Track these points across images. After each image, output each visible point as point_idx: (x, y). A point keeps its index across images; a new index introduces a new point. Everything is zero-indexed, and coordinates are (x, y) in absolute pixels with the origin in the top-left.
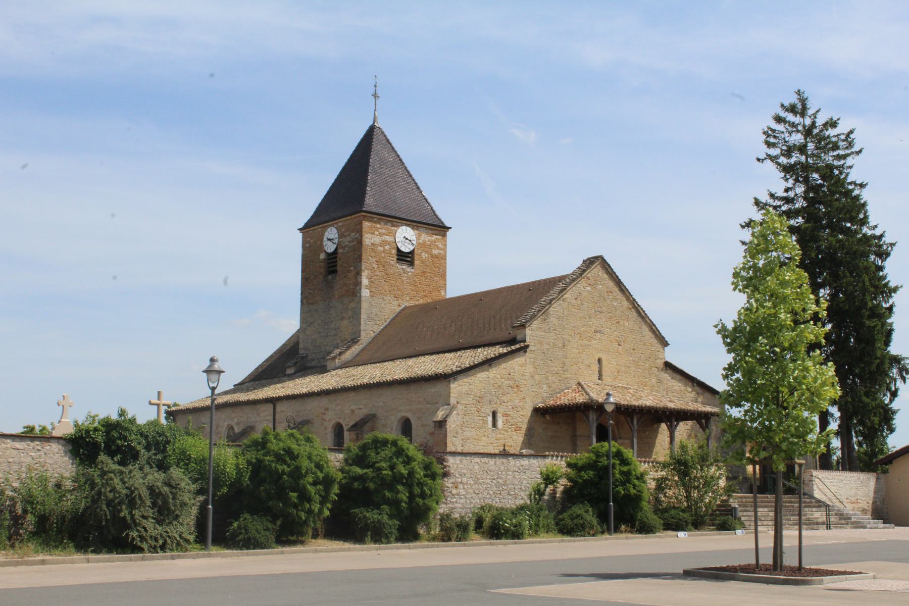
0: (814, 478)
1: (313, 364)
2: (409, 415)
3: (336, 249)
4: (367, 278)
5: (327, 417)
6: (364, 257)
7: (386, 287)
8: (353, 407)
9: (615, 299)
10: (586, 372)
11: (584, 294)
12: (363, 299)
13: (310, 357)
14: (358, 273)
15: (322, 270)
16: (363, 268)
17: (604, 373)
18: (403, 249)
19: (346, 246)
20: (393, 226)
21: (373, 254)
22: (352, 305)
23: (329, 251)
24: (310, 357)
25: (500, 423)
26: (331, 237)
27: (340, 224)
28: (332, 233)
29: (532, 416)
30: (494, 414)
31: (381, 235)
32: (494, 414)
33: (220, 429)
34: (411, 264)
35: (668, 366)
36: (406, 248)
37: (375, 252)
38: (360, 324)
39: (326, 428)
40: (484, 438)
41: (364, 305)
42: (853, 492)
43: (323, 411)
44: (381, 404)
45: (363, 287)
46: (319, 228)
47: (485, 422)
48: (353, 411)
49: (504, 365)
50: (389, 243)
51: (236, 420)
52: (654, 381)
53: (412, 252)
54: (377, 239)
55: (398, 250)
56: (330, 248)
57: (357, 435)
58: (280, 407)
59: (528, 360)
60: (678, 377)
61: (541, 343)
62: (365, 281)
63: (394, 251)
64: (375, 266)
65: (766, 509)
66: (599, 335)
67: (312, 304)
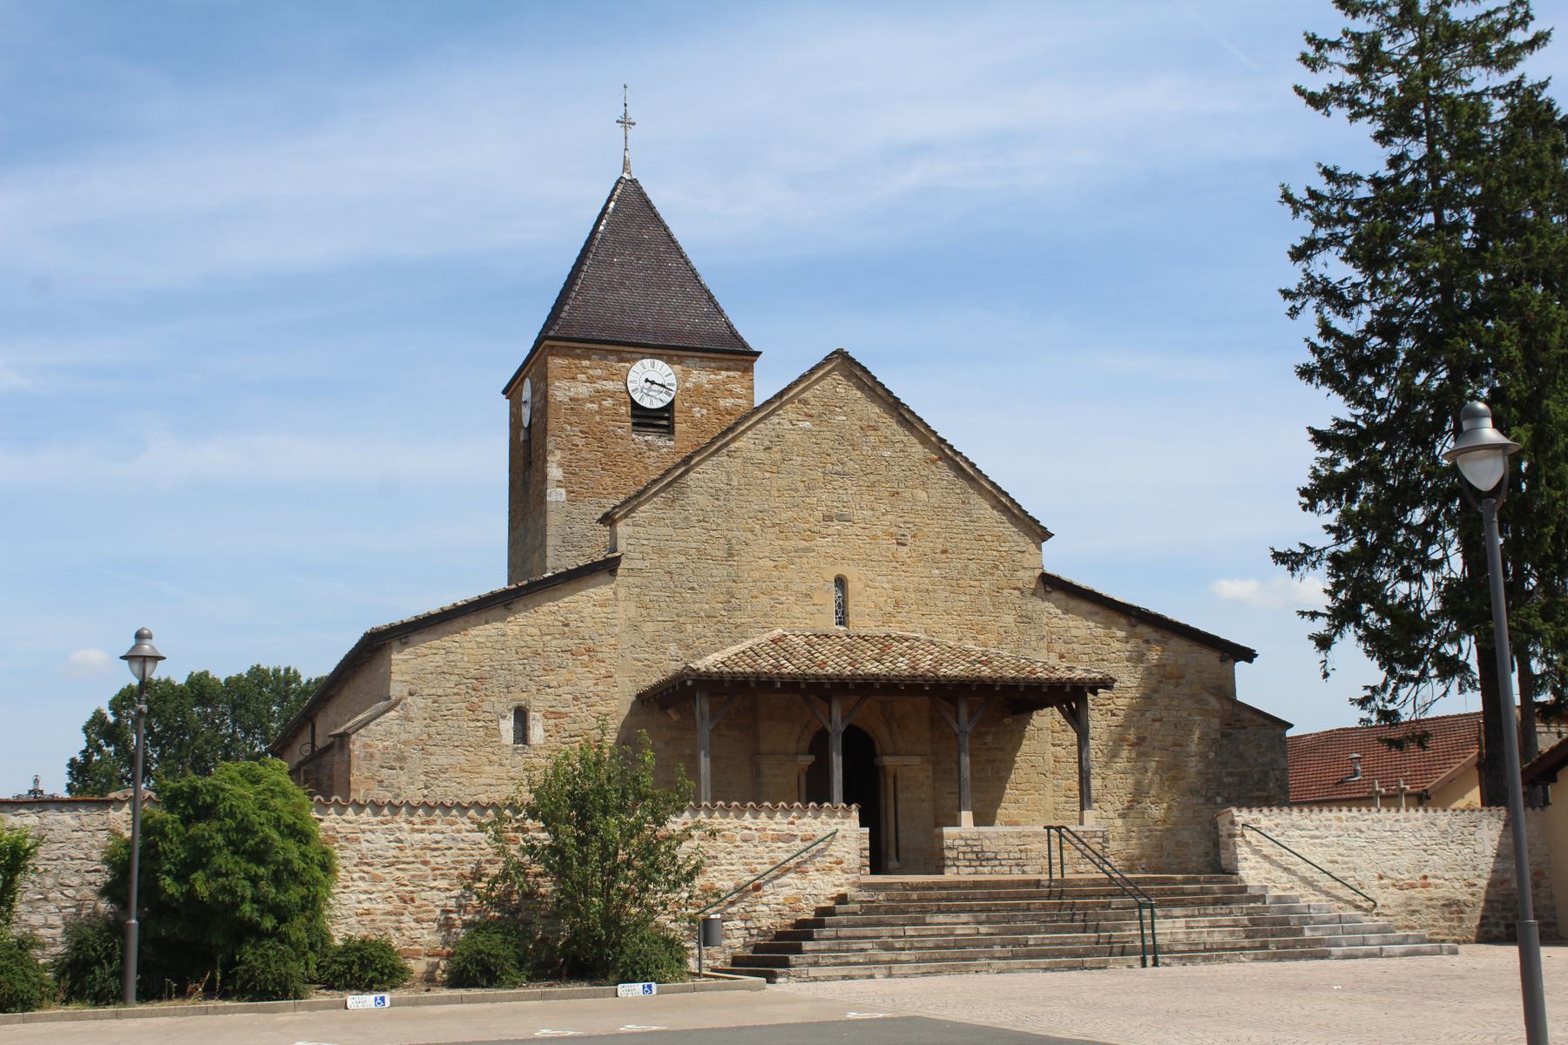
4: (560, 465)
10: (797, 609)
16: (550, 446)
17: (852, 608)
18: (646, 403)
20: (622, 360)
21: (574, 419)
25: (537, 733)
30: (521, 715)
31: (592, 380)
32: (521, 715)
34: (669, 430)
35: (1051, 584)
36: (653, 402)
37: (579, 414)
42: (1407, 859)
47: (493, 733)
49: (549, 606)
50: (612, 395)
52: (1009, 619)
53: (670, 407)
54: (582, 389)
59: (622, 592)
60: (1085, 607)
61: (660, 551)
62: (554, 472)
64: (580, 442)
65: (964, 917)
66: (836, 526)
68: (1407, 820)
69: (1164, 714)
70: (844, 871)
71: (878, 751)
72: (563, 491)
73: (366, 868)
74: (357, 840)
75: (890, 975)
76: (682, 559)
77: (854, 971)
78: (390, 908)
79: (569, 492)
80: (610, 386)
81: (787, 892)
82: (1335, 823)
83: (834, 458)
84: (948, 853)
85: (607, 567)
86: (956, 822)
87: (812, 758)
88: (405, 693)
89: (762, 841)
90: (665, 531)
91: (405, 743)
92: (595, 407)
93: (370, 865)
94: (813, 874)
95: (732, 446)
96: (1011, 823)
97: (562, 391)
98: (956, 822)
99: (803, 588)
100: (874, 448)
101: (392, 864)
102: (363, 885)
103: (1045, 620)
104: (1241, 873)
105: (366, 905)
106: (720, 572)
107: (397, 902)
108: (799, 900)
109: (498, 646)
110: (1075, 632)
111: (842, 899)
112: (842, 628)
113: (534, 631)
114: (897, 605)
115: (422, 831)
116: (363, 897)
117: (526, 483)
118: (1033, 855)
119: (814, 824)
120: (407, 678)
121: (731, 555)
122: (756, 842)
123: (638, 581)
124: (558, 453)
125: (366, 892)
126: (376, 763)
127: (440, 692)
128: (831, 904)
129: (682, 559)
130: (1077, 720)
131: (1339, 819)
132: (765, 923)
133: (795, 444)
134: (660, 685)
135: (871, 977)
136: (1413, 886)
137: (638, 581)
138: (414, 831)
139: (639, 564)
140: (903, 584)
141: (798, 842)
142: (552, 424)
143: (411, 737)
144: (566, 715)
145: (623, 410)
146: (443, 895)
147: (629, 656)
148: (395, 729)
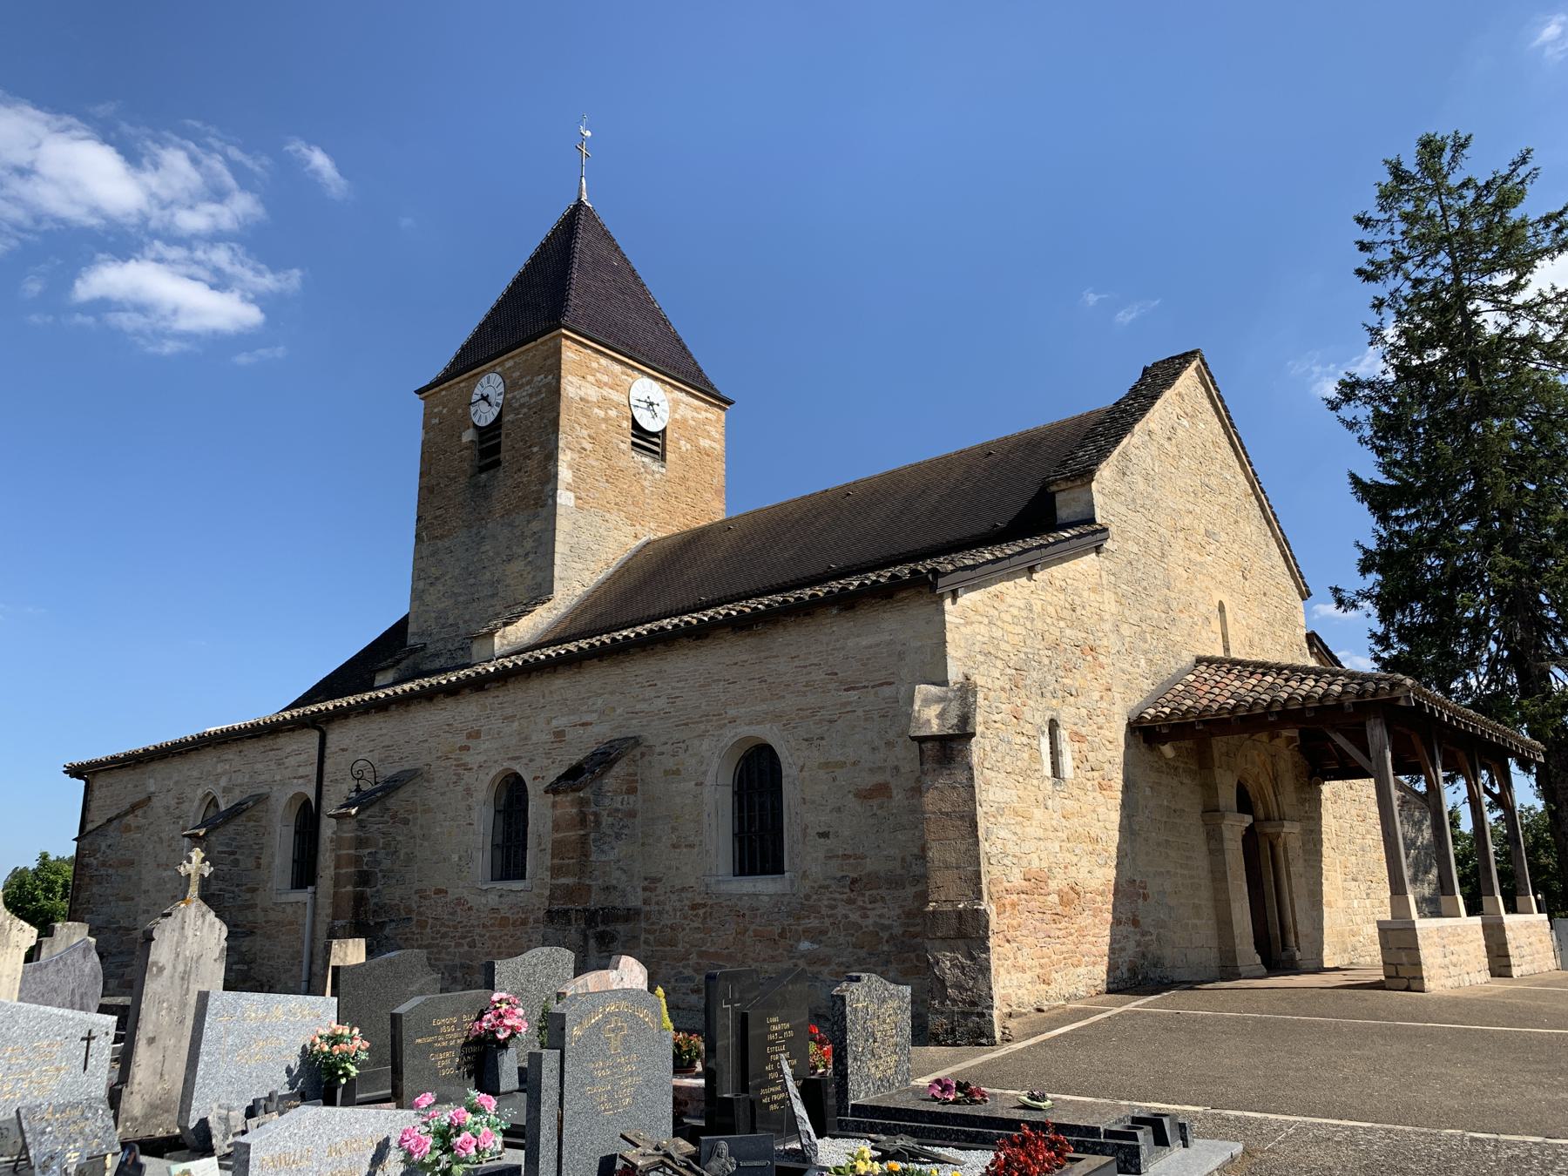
1: (437, 664)
2: (768, 733)
3: (500, 413)
4: (570, 467)
5: (471, 759)
6: (563, 420)
7: (610, 495)
8: (560, 722)
11: (1180, 432)
12: (560, 511)
13: (431, 649)
14: (551, 457)
15: (466, 465)
16: (561, 444)
19: (522, 405)
21: (584, 421)
22: (536, 526)
23: (483, 424)
24: (431, 649)
26: (489, 392)
27: (509, 364)
28: (491, 385)
29: (1127, 746)
32: (1053, 725)
33: (185, 806)
37: (587, 416)
38: (553, 564)
39: (468, 792)
41: (563, 525)
43: (461, 740)
44: (661, 703)
45: (561, 485)
46: (460, 382)
48: (559, 734)
50: (617, 406)
51: (223, 782)
53: (664, 431)
54: (592, 393)
56: (484, 415)
57: (582, 803)
58: (339, 737)
62: (565, 474)
63: (627, 424)
64: (589, 446)
67: (442, 537)
72: (572, 495)
79: (578, 498)
92: (602, 414)
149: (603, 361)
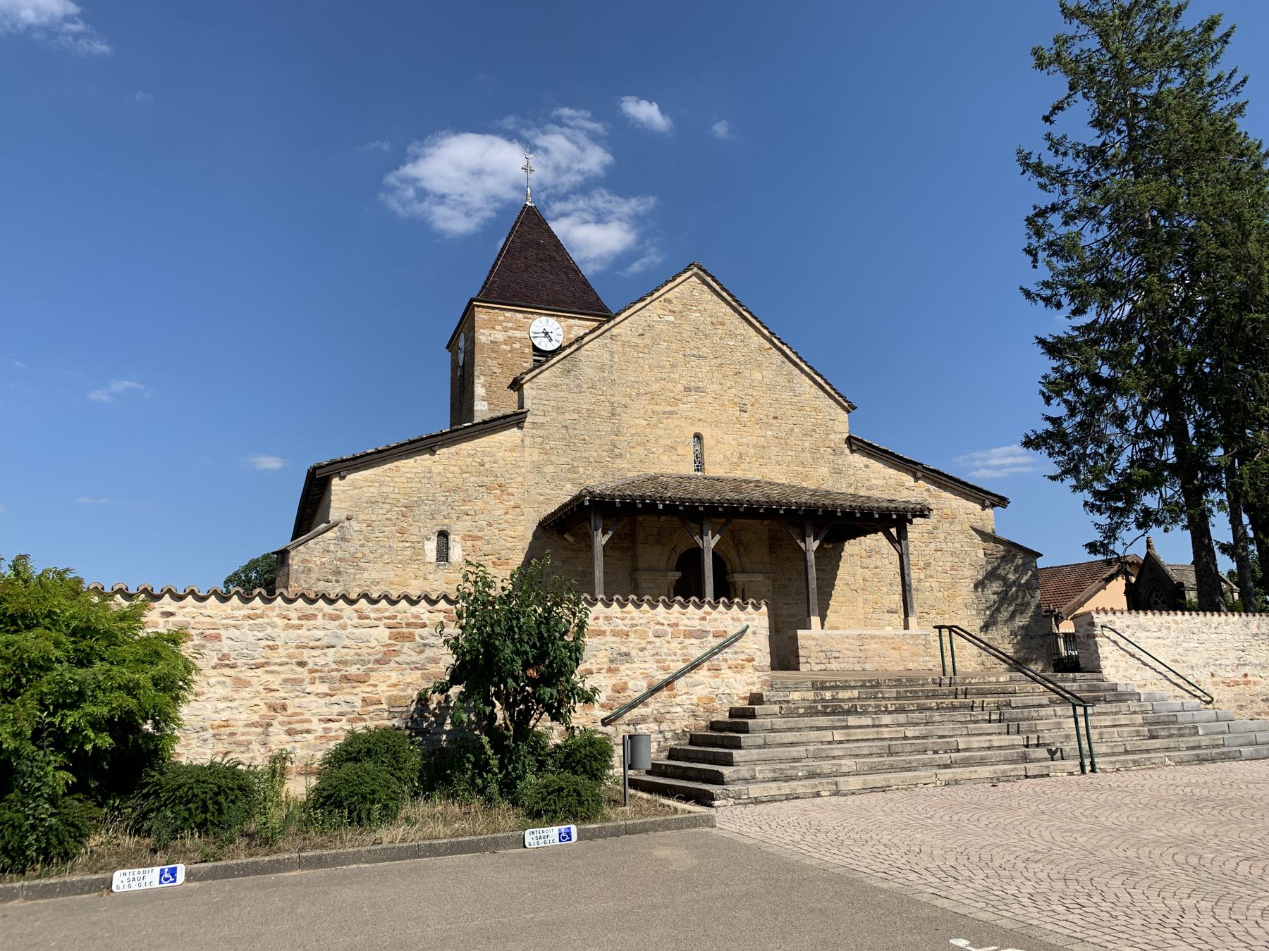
0: (1098, 631)
4: (484, 386)
9: (732, 335)
10: (664, 458)
11: (659, 327)
16: (476, 373)
30: (443, 535)
31: (505, 329)
32: (443, 535)
40: (414, 582)
50: (520, 340)
54: (499, 336)
55: (535, 348)
59: (528, 441)
62: (479, 390)
63: (529, 351)
66: (693, 396)
68: (1227, 624)
69: (944, 545)
70: (756, 669)
71: (729, 570)
73: (227, 671)
74: (218, 638)
75: (836, 793)
76: (576, 416)
77: (800, 787)
78: (255, 718)
80: (518, 334)
81: (702, 691)
82: (1173, 626)
83: (692, 344)
84: (801, 652)
85: (516, 419)
86: (807, 626)
87: (679, 574)
88: (343, 517)
89: (674, 636)
90: (562, 394)
91: (340, 560)
92: (508, 348)
93: (233, 667)
94: (725, 672)
95: (615, 331)
96: (831, 628)
97: (483, 336)
98: (807, 626)
99: (669, 442)
100: (721, 339)
101: (262, 665)
102: (221, 691)
103: (852, 472)
104: (1105, 672)
105: (226, 715)
106: (605, 428)
107: (264, 710)
108: (712, 700)
109: (425, 481)
110: (874, 481)
111: (756, 699)
112: (699, 474)
113: (456, 469)
114: (741, 457)
115: (299, 627)
116: (221, 705)
117: (461, 403)
118: (869, 654)
119: (726, 618)
120: (344, 505)
121: (614, 414)
122: (669, 638)
123: (541, 432)
124: (482, 378)
125: (225, 699)
126: (314, 576)
127: (374, 518)
128: (743, 704)
129: (576, 416)
130: (898, 541)
131: (1176, 622)
132: (680, 726)
133: (662, 331)
134: (560, 509)
135: (818, 795)
136: (1237, 684)
137: (541, 432)
138: (288, 627)
139: (541, 419)
140: (745, 441)
141: (710, 637)
142: (478, 358)
143: (347, 555)
144: (481, 538)
145: (527, 350)
146: (323, 701)
147: (533, 491)
148: (332, 548)
149: (508, 314)
